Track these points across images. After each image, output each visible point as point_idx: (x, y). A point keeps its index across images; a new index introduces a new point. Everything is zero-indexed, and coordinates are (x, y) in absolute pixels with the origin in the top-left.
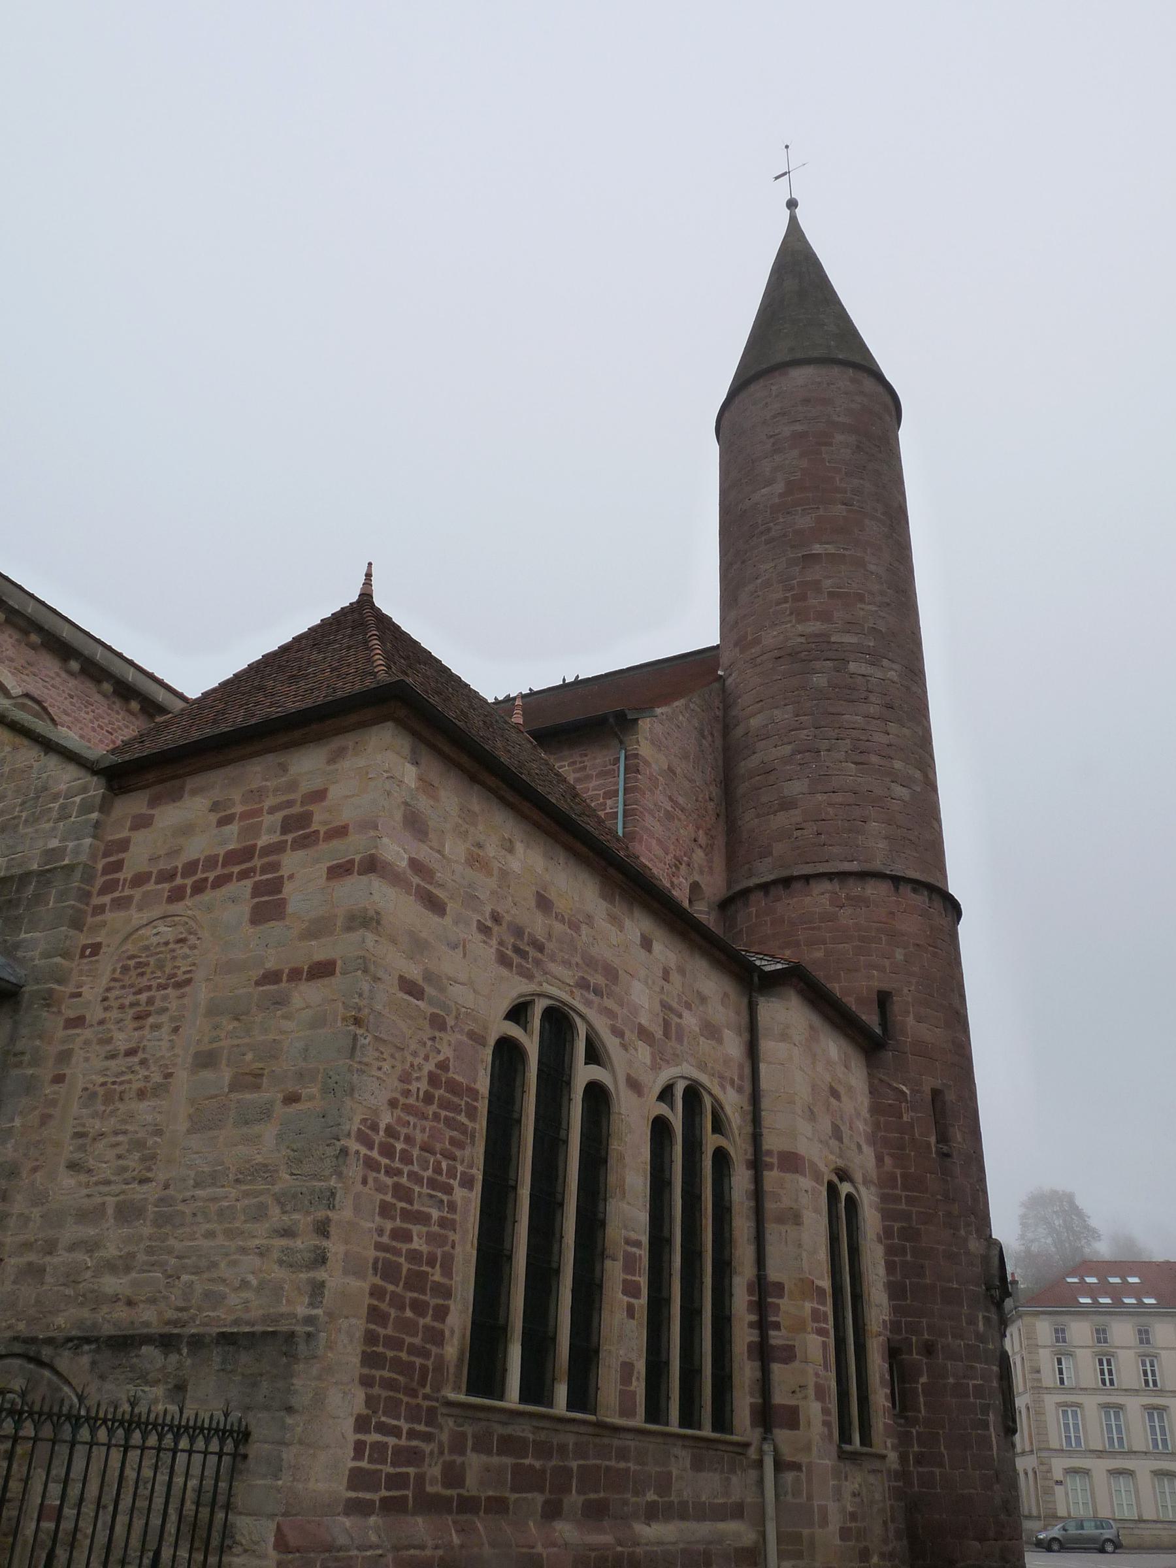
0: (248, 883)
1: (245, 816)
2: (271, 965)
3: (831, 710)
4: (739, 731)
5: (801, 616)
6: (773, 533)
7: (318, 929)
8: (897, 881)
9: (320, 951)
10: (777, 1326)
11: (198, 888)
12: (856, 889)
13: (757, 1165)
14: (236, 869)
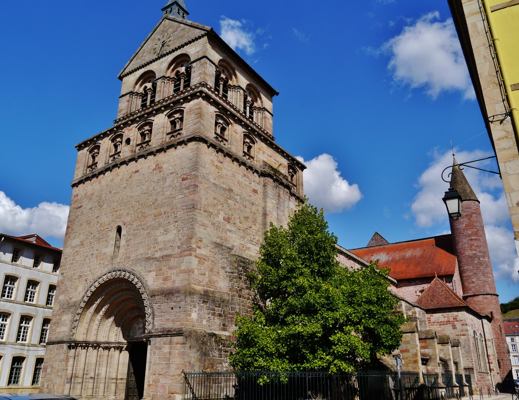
2: (457, 334)
4: (462, 268)
5: (471, 250)
7: (462, 331)
8: (491, 295)
9: (463, 333)
11: (443, 324)
12: (485, 296)
13: (485, 341)
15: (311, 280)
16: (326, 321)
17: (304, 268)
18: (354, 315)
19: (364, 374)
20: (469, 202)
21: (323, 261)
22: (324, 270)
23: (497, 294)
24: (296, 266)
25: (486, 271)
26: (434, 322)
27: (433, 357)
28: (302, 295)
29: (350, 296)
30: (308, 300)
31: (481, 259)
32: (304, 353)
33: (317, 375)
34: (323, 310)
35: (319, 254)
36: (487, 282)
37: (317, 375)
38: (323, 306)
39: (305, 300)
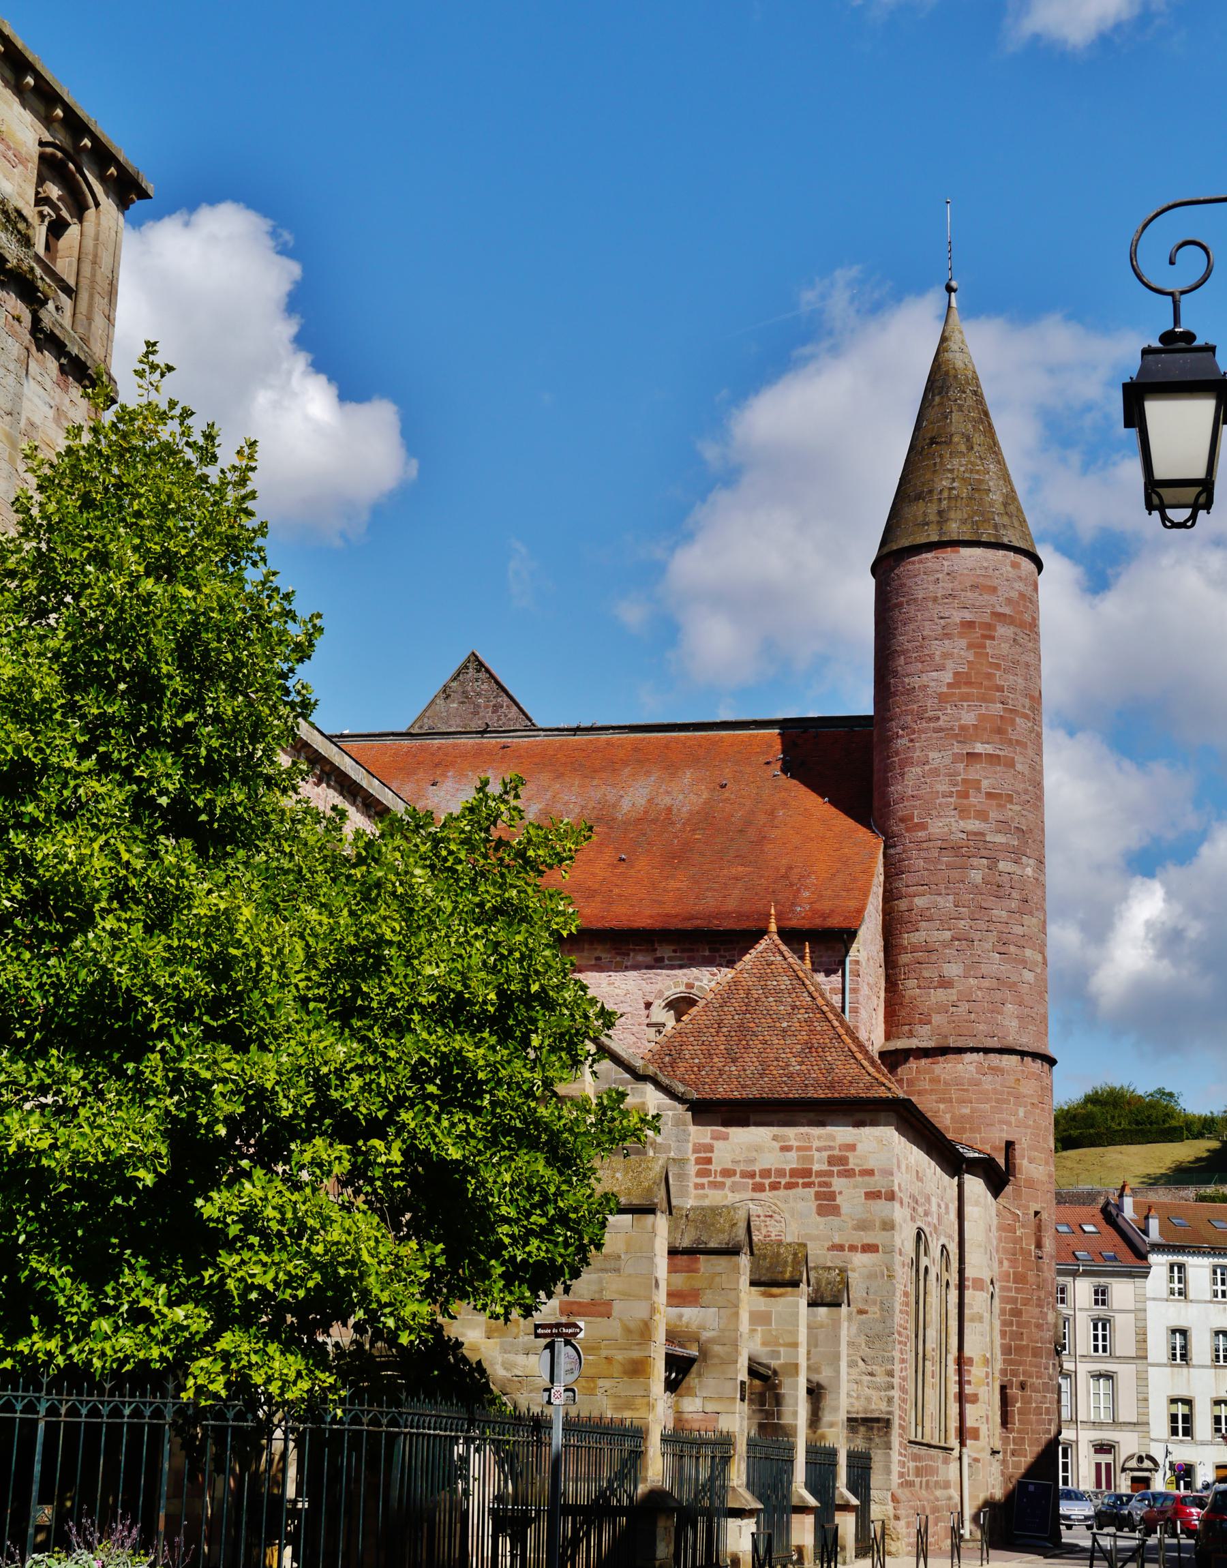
0: (812, 1191)
1: (799, 1149)
2: (837, 1240)
3: (984, 905)
4: (903, 905)
5: (963, 812)
6: (941, 723)
7: (863, 1226)
8: (1023, 1054)
9: (869, 1238)
10: (969, 1382)
11: (775, 1187)
13: (961, 1288)
14: (801, 1181)
15: (133, 854)
16: (194, 1101)
17: (90, 772)
18: (356, 1082)
19: (375, 1422)
20: (990, 553)
21: (215, 743)
22: (210, 803)
23: (1052, 1052)
24: (44, 760)
25: (1018, 930)
26: (727, 1173)
27: (717, 1349)
28: (64, 939)
29: (340, 969)
30: (104, 969)
31: (1002, 865)
32: (35, 1275)
33: (105, 1411)
34: (183, 1036)
35: (194, 702)
36: (1013, 987)
37: (105, 1411)
38: (184, 1012)
39: (84, 964)
